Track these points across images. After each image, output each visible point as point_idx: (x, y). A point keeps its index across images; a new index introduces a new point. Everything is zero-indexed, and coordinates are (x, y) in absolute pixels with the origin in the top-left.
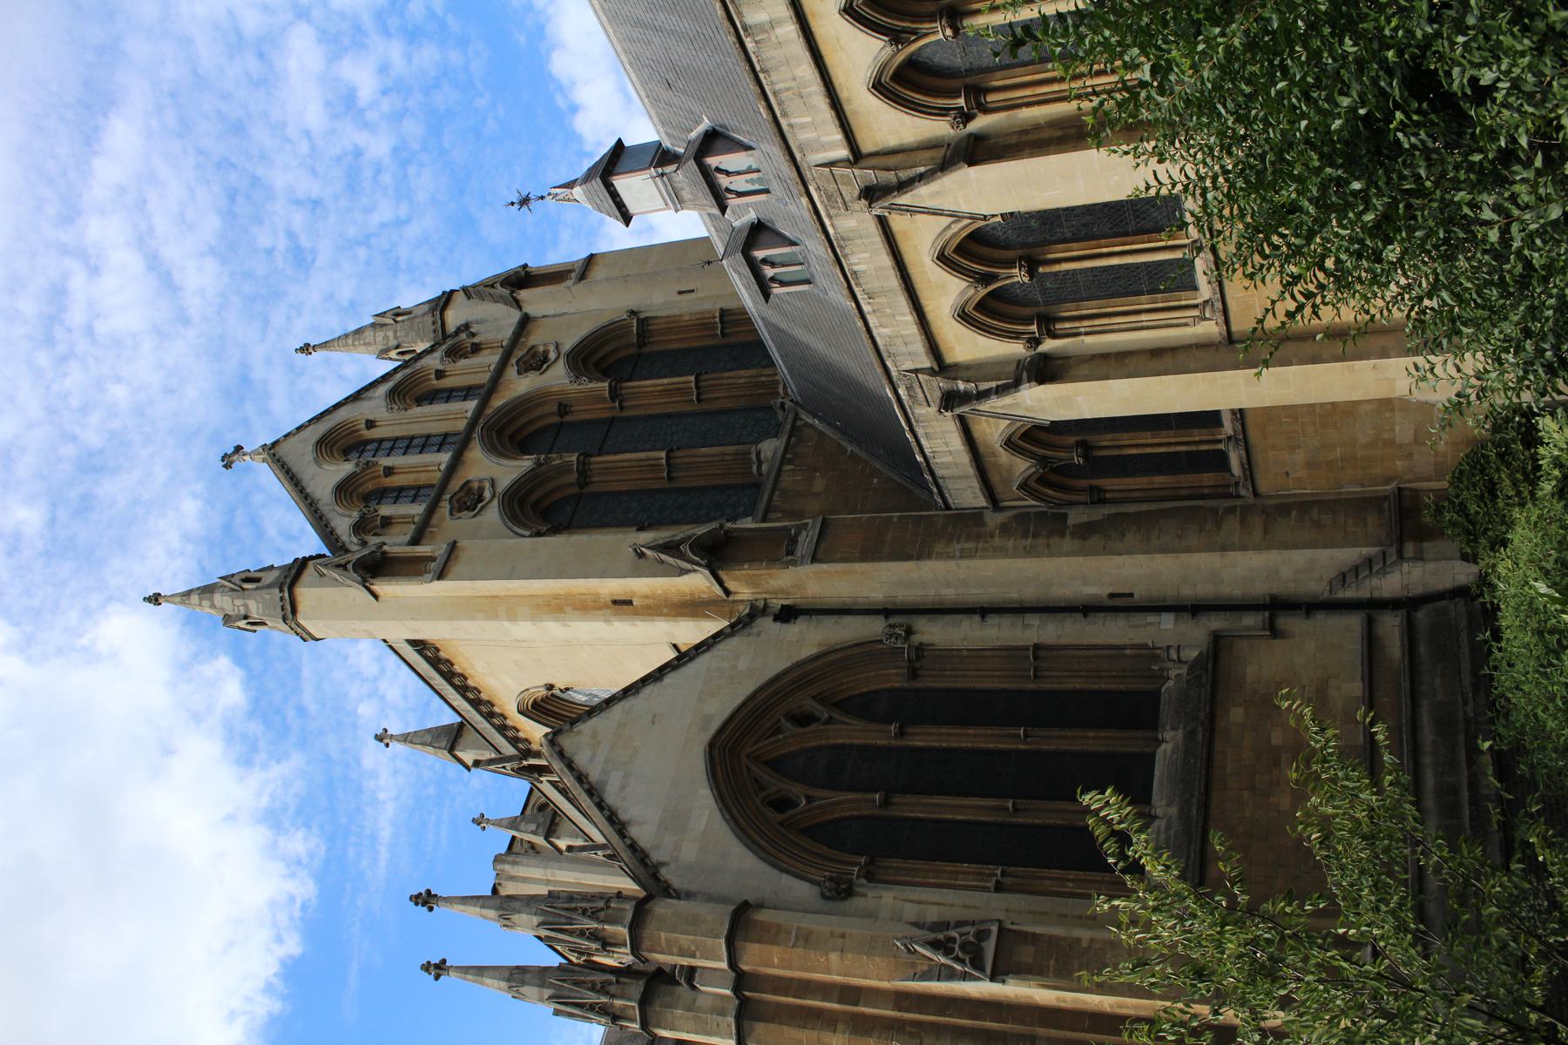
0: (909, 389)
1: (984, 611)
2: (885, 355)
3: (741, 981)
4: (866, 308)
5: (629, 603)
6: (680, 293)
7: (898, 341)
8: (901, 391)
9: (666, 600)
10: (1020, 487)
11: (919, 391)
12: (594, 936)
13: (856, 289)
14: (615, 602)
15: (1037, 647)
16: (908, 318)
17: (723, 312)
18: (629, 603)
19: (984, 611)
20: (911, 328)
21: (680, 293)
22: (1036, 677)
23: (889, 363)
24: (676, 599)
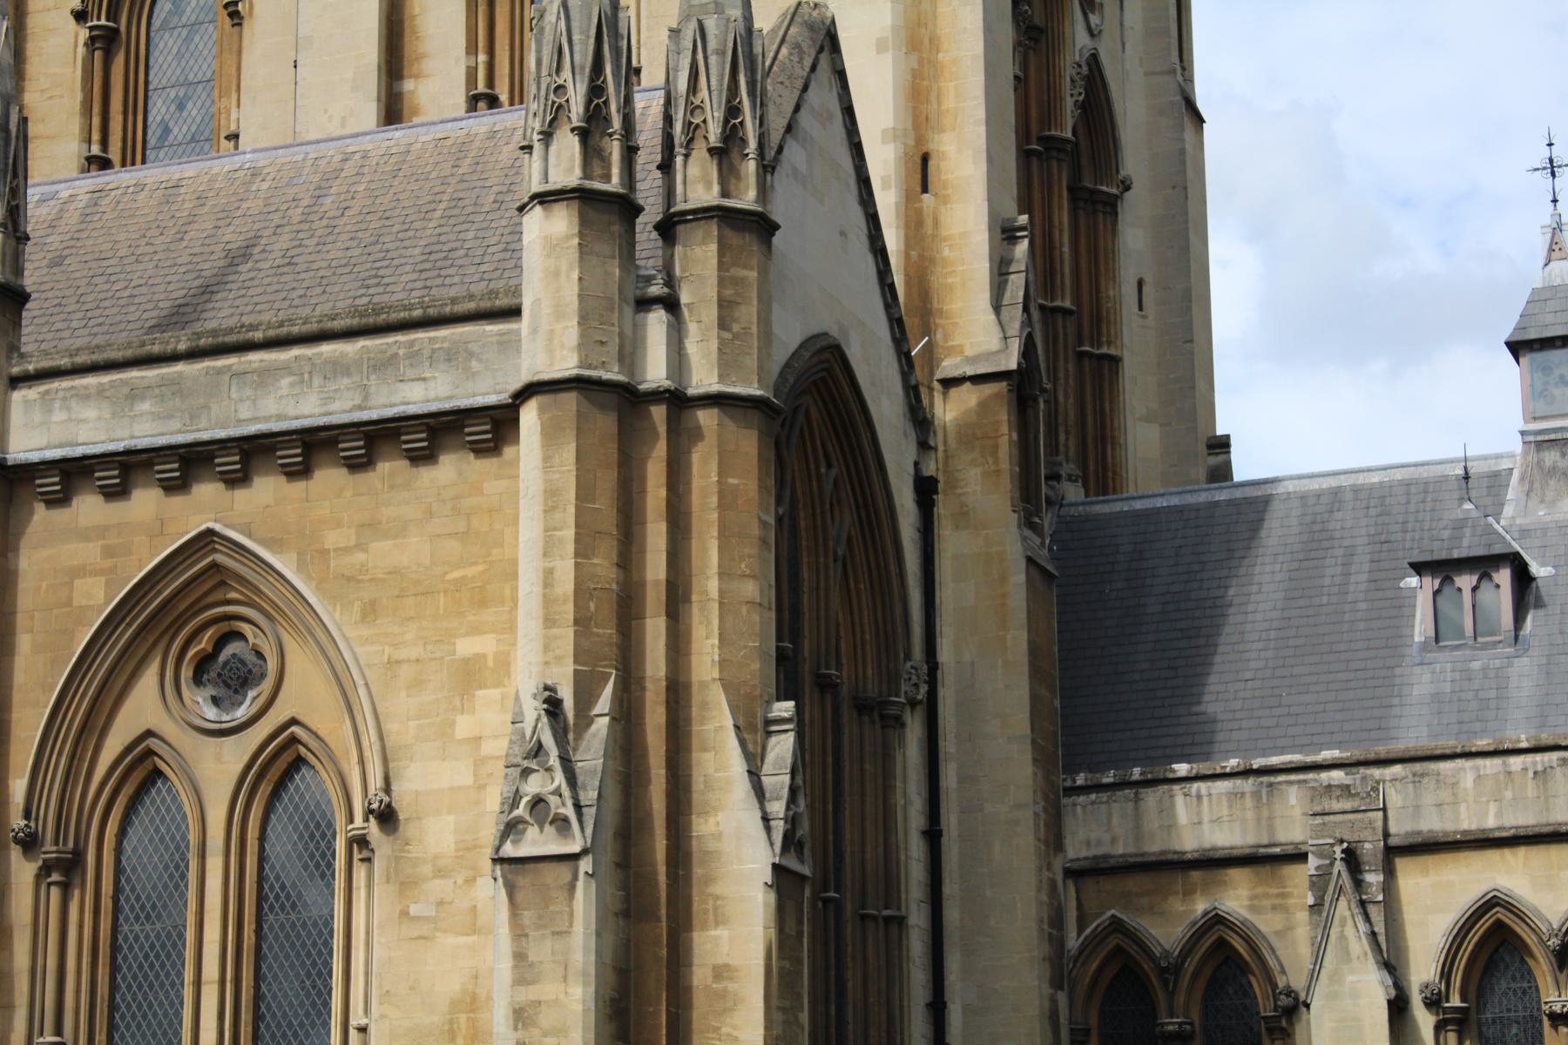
0: (1346, 790)
1: (933, 835)
2: (1418, 767)
3: (678, 401)
4: (1516, 762)
5: (925, 189)
6: (1140, 283)
7: (1445, 795)
8: (1337, 776)
9: (932, 260)
10: (1116, 925)
11: (1348, 805)
12: (732, 135)
13: (1554, 756)
14: (925, 159)
15: (901, 921)
16: (1491, 820)
17: (1115, 361)
18: (925, 189)
19: (933, 835)
20: (1467, 821)
21: (1140, 283)
22: (864, 918)
23: (1397, 769)
24: (936, 280)
